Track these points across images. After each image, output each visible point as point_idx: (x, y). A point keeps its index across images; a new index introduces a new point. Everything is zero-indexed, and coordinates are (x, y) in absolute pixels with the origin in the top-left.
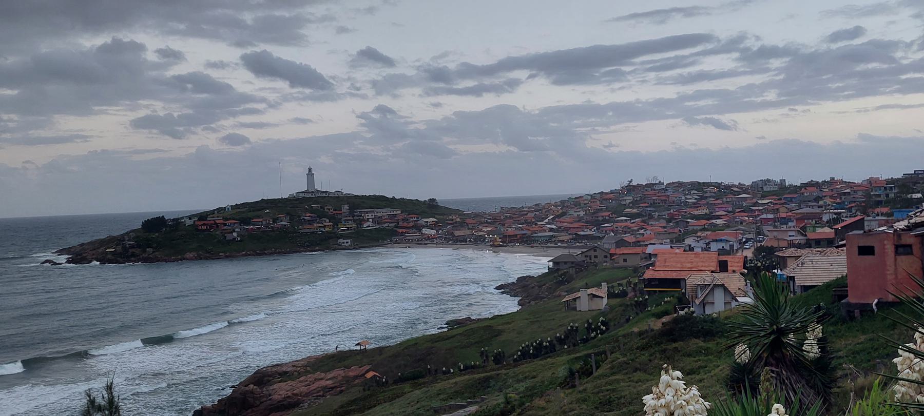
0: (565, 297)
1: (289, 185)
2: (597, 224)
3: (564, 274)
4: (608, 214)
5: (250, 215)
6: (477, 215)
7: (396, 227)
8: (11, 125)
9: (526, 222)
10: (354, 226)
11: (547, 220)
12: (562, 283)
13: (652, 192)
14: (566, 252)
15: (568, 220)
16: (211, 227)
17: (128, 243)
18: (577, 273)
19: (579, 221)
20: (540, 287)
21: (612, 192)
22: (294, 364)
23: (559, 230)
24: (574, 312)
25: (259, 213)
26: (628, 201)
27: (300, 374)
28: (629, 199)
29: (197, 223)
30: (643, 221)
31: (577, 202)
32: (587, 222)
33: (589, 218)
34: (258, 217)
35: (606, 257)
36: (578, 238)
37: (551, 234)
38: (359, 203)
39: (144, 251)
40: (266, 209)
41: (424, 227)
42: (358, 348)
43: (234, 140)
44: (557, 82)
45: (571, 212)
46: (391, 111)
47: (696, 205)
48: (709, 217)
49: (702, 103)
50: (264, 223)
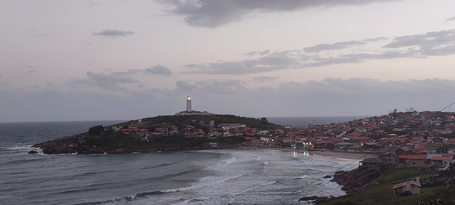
6: (294, 130)
7: (245, 135)
9: (328, 135)
11: (342, 134)
17: (81, 142)
19: (364, 136)
25: (159, 125)
26: (395, 123)
28: (396, 122)
29: (122, 130)
30: (407, 137)
32: (369, 136)
34: (159, 127)
40: (163, 122)
41: (262, 136)
45: (357, 129)
47: (442, 127)
50: (163, 131)
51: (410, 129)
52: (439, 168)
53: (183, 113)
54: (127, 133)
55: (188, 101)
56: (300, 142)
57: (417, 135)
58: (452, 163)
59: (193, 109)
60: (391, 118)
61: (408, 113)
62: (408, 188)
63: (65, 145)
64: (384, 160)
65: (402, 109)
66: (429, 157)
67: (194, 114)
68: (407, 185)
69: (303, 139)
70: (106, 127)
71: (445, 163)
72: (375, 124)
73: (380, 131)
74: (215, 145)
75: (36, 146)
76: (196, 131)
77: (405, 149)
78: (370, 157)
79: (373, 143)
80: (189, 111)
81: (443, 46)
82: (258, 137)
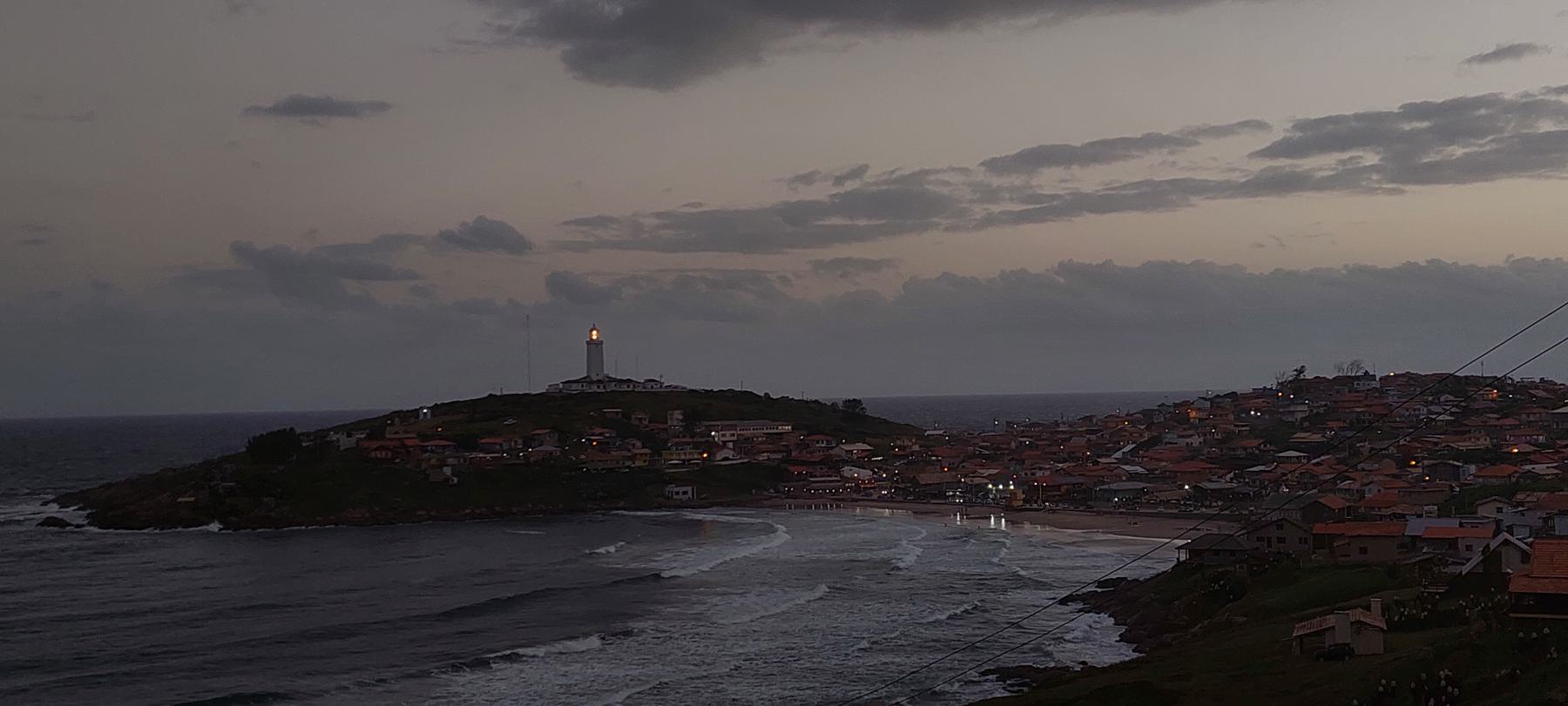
4: (1255, 443)
7: (783, 461)
9: (1071, 457)
11: (1118, 455)
19: (1192, 458)
21: (1262, 393)
26: (1299, 416)
28: (1301, 410)
29: (366, 444)
41: (846, 462)
47: (1458, 428)
48: (1493, 456)
50: (505, 447)
51: (1349, 434)
52: (1446, 565)
53: (574, 386)
55: (591, 342)
56: (977, 481)
57: (1375, 455)
58: (1493, 546)
59: (610, 370)
62: (1343, 636)
65: (1322, 366)
66: (1415, 527)
67: (612, 387)
68: (1338, 625)
69: (986, 473)
70: (308, 435)
71: (1469, 548)
72: (1232, 417)
73: (1245, 443)
74: (685, 493)
75: (63, 502)
76: (619, 448)
77: (1334, 501)
78: (1215, 531)
79: (1226, 482)
80: (595, 378)
81: (1458, 151)
82: (834, 465)
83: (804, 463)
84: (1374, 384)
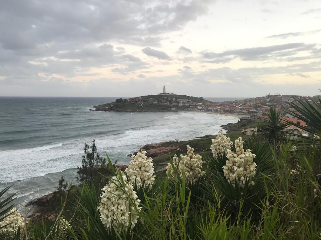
0: (243, 130)
1: (157, 91)
2: (256, 108)
3: (244, 123)
4: (260, 104)
5: (146, 99)
8: (79, 70)
9: (232, 106)
10: (176, 104)
11: (239, 106)
12: (242, 126)
13: (277, 98)
14: (245, 116)
15: (247, 106)
16: (135, 102)
18: (248, 123)
19: (250, 107)
20: (235, 127)
21: (262, 97)
22: (156, 144)
23: (243, 109)
24: (245, 136)
25: (148, 99)
26: (268, 101)
27: (158, 147)
28: (268, 100)
31: (250, 100)
33: (254, 106)
34: (149, 100)
35: (258, 118)
36: (249, 112)
37: (240, 110)
38: (179, 98)
39: (116, 108)
40: (151, 98)
41: (198, 106)
42: (175, 141)
43: (141, 76)
44: (244, 60)
46: (190, 68)
49: (295, 68)
54: (133, 102)
56: (216, 109)
60: (266, 98)
61: (276, 96)
63: (104, 107)
64: (252, 118)
65: (273, 94)
72: (257, 101)
73: (259, 105)
83: (192, 106)
84: (281, 96)
